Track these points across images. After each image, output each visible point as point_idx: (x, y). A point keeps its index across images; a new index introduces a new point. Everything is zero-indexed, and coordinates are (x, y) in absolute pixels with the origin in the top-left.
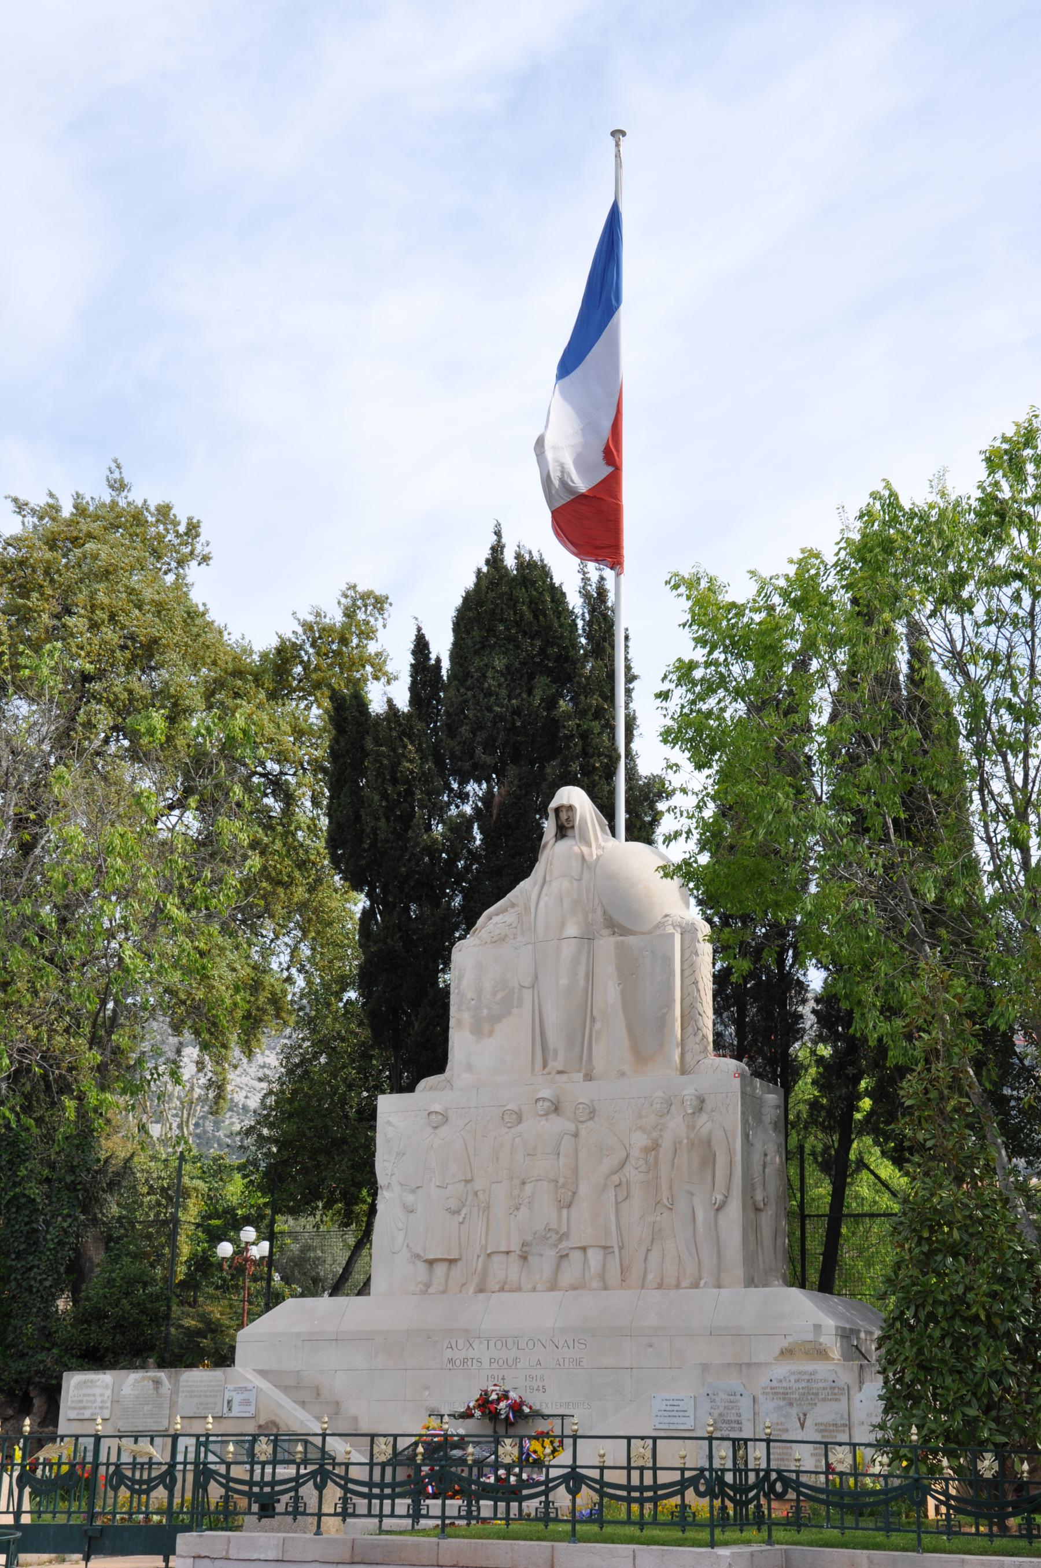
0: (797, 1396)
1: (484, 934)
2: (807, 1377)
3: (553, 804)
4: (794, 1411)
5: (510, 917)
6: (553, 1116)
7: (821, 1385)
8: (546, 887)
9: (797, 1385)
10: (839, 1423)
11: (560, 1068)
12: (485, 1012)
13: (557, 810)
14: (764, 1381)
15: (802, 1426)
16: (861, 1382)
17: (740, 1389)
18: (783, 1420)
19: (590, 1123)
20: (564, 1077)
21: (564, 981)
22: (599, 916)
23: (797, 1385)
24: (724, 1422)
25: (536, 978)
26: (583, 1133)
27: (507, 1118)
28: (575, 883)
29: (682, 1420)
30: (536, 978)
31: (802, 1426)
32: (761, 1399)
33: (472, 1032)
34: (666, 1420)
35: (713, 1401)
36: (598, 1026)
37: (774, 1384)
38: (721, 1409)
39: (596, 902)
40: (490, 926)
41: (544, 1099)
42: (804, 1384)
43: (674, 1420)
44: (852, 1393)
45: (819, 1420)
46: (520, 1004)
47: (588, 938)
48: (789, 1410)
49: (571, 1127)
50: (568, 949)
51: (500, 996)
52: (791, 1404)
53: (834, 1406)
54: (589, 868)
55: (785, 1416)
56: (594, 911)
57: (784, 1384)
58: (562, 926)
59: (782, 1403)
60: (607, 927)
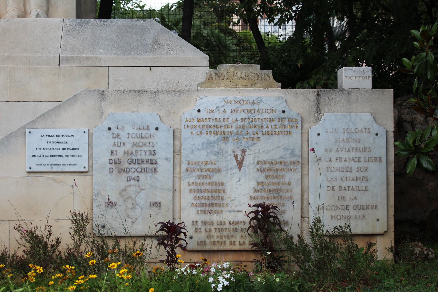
0: (234, 130)
2: (248, 107)
4: (229, 147)
7: (267, 116)
9: (234, 116)
10: (288, 160)
14: (189, 112)
15: (240, 164)
16: (319, 112)
17: (154, 122)
18: (213, 158)
23: (234, 116)
24: (132, 162)
29: (71, 160)
31: (240, 164)
32: (186, 133)
34: (48, 161)
35: (118, 136)
37: (203, 115)
38: (128, 147)
42: (243, 115)
43: (60, 161)
44: (305, 126)
45: (263, 157)
48: (223, 146)
52: (225, 139)
53: (284, 140)
55: (217, 154)
57: (217, 115)
59: (213, 138)
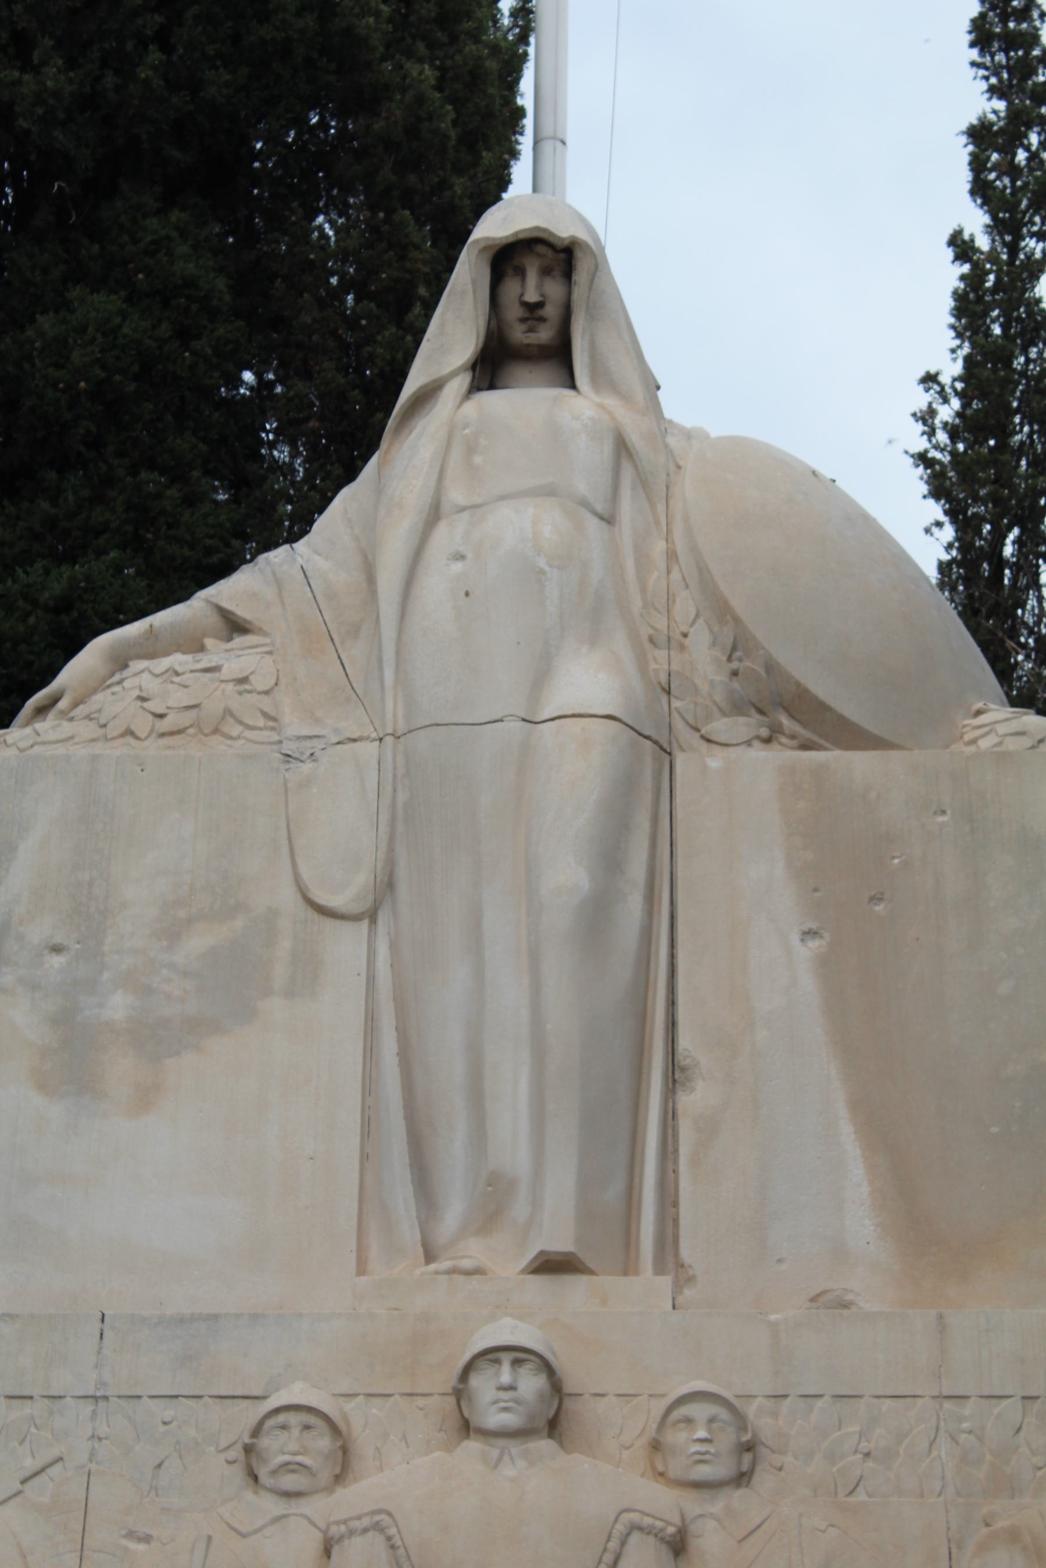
1: (116, 704)
3: (494, 226)
5: (235, 658)
6: (544, 1445)
8: (443, 538)
11: (559, 1240)
12: (118, 1006)
13: (506, 258)
19: (738, 1497)
20: (575, 1286)
21: (567, 874)
22: (703, 662)
25: (390, 885)
26: (711, 1541)
27: (278, 1448)
28: (593, 524)
30: (386, 886)
33: (42, 1087)
36: (688, 1101)
39: (685, 605)
40: (142, 675)
41: (520, 1355)
46: (307, 975)
47: (652, 745)
49: (663, 1503)
50: (576, 773)
51: (198, 943)
54: (643, 482)
56: (676, 642)
58: (541, 675)
60: (737, 707)
